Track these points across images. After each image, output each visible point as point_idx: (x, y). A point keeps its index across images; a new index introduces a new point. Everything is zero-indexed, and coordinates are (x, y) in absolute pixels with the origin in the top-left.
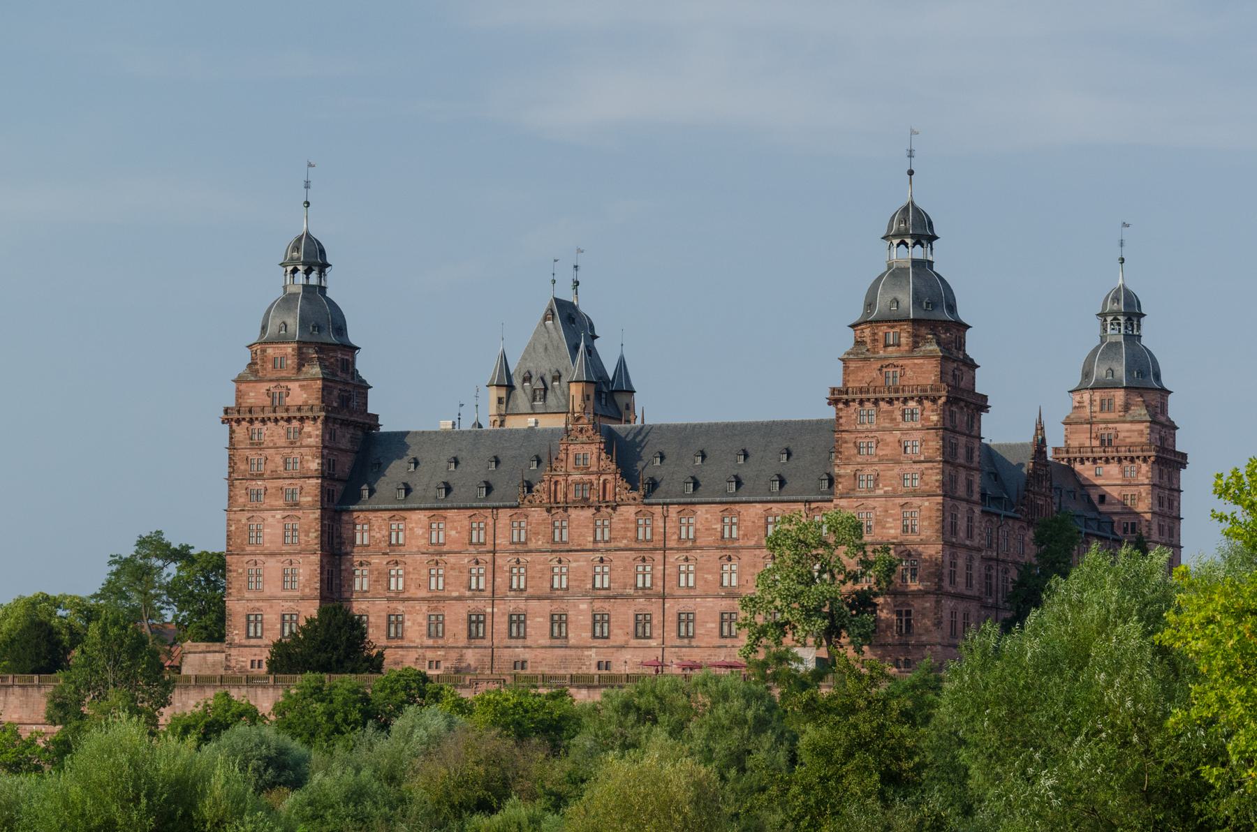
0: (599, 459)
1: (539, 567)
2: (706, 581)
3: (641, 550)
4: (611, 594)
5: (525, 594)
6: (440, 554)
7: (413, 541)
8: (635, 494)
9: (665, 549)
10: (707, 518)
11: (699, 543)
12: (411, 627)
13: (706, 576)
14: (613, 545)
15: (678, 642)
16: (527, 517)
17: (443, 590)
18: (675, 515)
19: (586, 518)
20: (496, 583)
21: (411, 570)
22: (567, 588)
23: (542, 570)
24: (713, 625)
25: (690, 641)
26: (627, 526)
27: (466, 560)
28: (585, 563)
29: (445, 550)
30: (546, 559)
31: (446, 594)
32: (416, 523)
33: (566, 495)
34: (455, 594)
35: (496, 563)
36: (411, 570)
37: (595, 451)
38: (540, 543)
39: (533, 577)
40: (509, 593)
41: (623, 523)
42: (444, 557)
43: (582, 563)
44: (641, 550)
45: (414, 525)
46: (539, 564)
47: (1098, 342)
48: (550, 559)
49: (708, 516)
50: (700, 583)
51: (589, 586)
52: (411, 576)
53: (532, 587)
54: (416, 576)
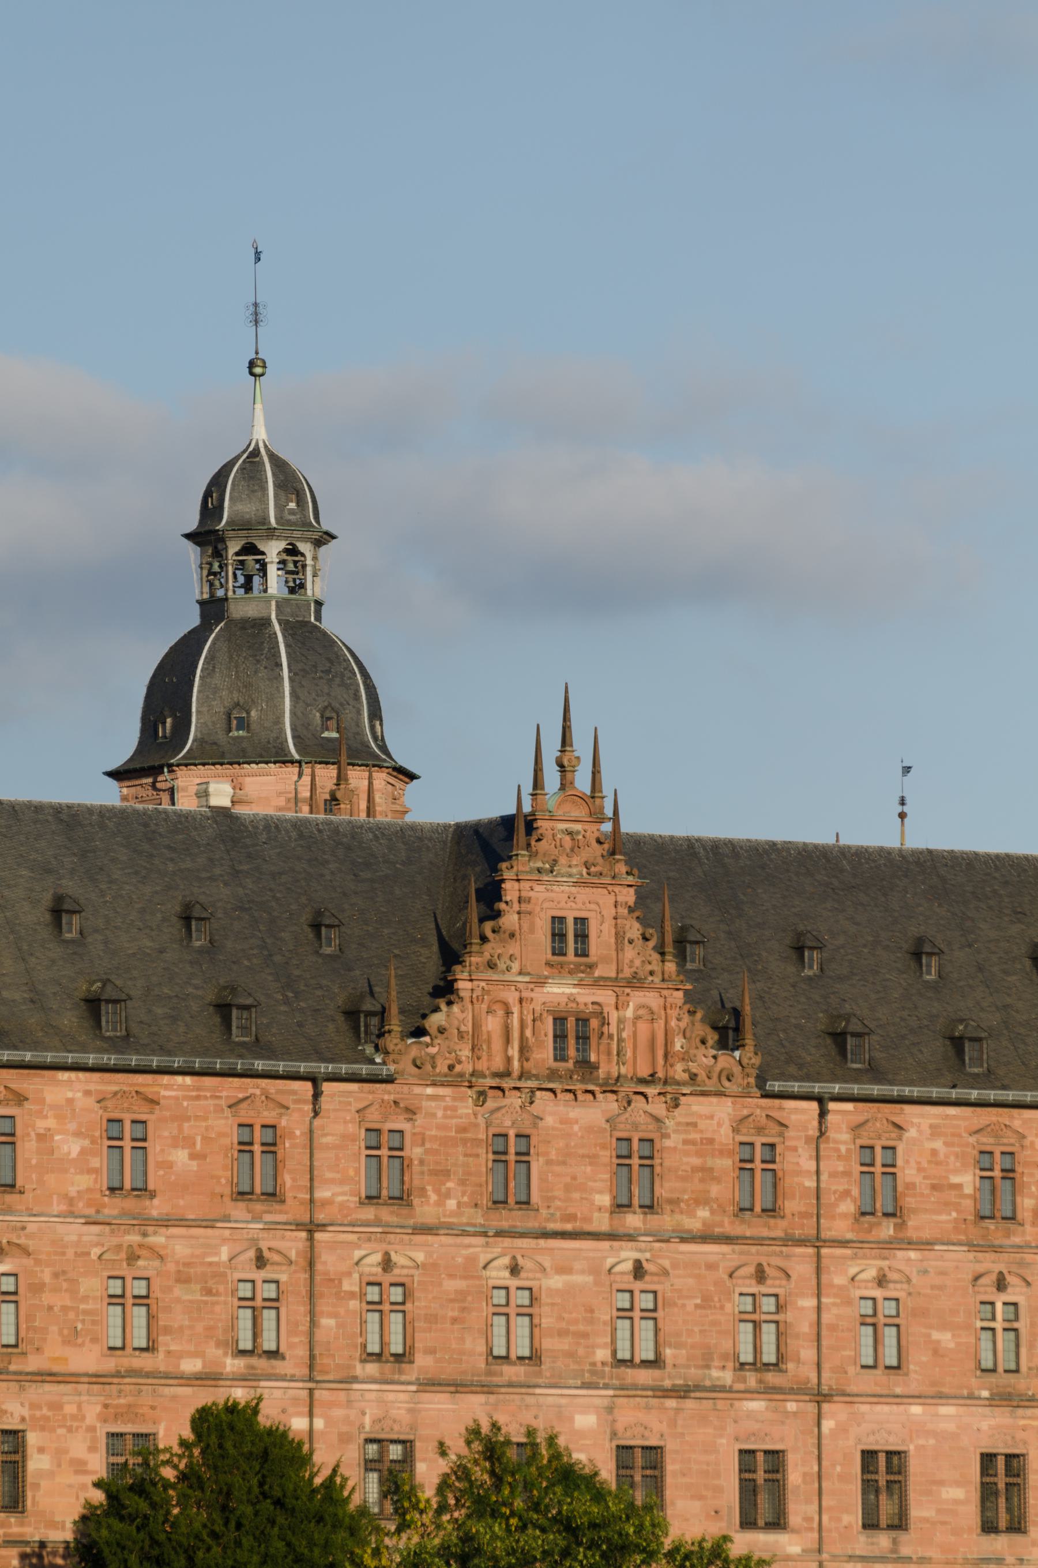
0: (619, 936)
1: (452, 1285)
2: (937, 1351)
3: (759, 1241)
4: (667, 1383)
5: (411, 1372)
6: (145, 1223)
7: (51, 1179)
8: (726, 1061)
9: (817, 1242)
10: (934, 1152)
11: (917, 1225)
12: (51, 1474)
13: (936, 1335)
14: (666, 1221)
15: (862, 1543)
16: (411, 1112)
17: (149, 1348)
18: (846, 1137)
19: (589, 1129)
20: (320, 1335)
21: (47, 1276)
22: (534, 1358)
23: (461, 1296)
24: (957, 1493)
25: (895, 1542)
26: (710, 1163)
27: (224, 1254)
28: (589, 1279)
29: (155, 1213)
30: (472, 1260)
31: (156, 1362)
32: (60, 1118)
33: (524, 1049)
34: (191, 1366)
35: (319, 1267)
36: (47, 1276)
37: (609, 912)
38: (452, 1204)
39: (432, 1319)
40: (359, 1370)
41: (699, 1154)
42: (158, 1239)
43: (578, 1279)
44: (759, 1241)
45: (51, 1123)
46: (451, 1276)
47: (194, 620)
48: (483, 1259)
49: (938, 1144)
50: (918, 1359)
51: (602, 1354)
52: (47, 1298)
53: (431, 1351)
54: (59, 1300)
